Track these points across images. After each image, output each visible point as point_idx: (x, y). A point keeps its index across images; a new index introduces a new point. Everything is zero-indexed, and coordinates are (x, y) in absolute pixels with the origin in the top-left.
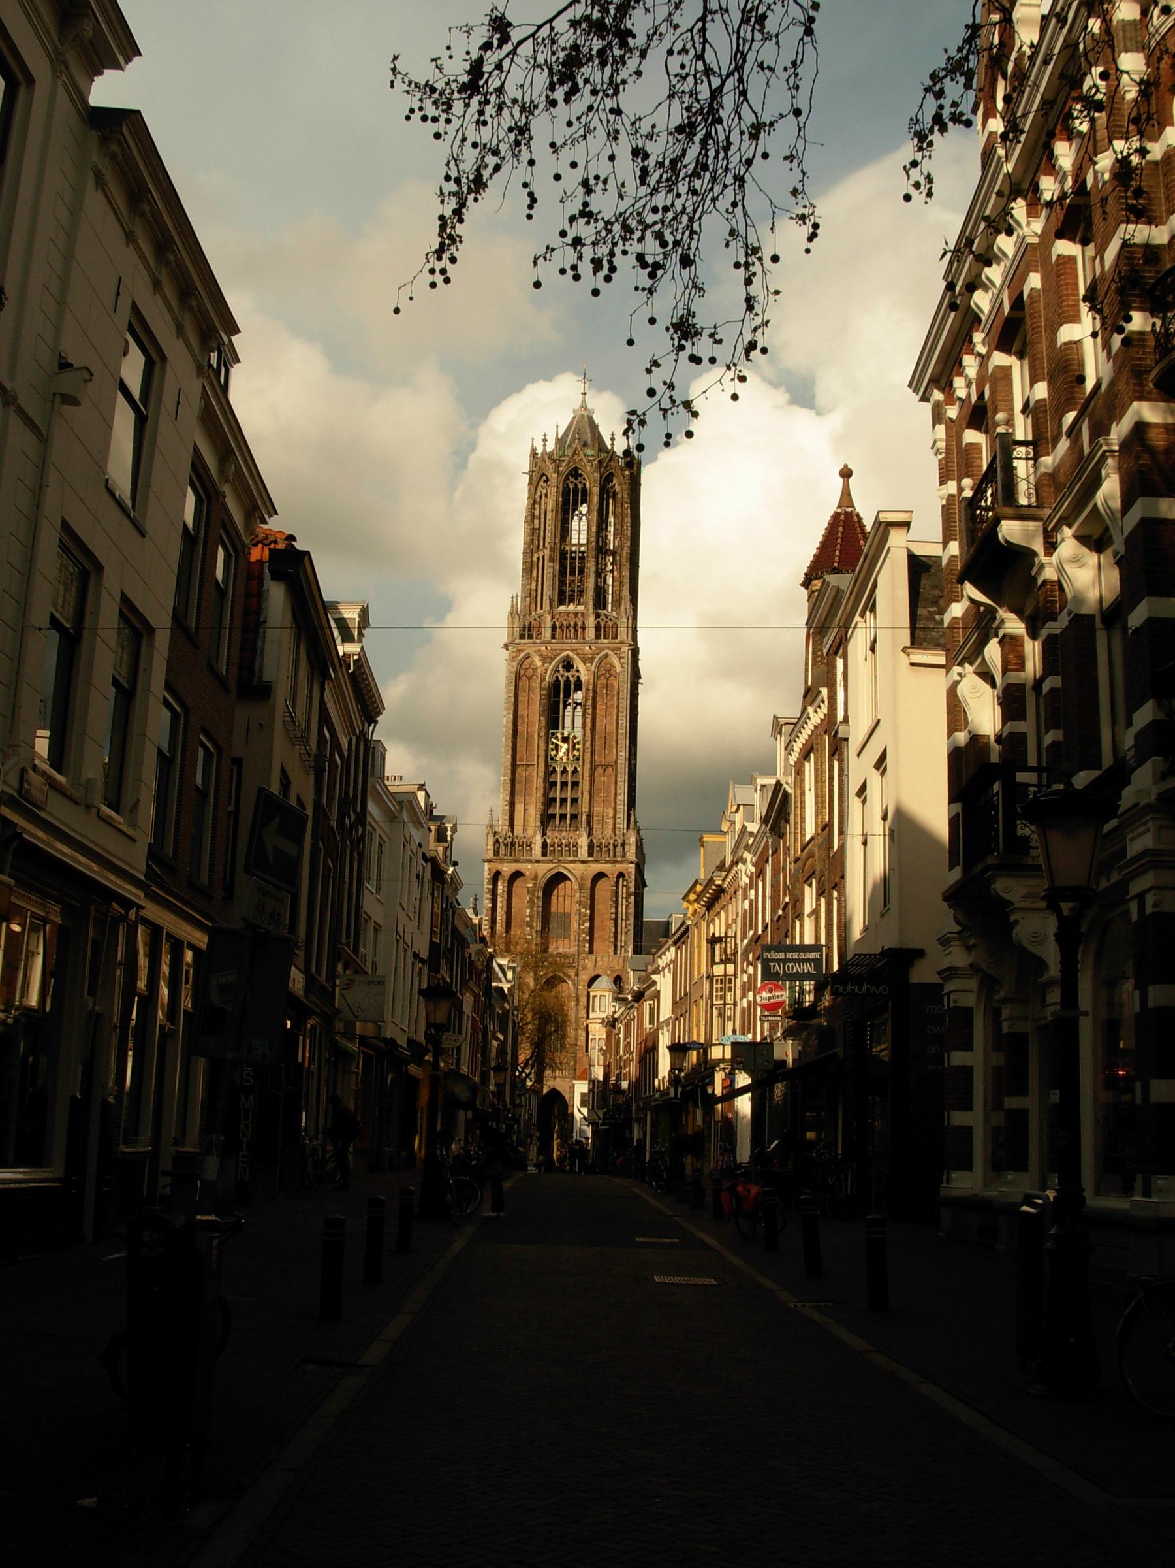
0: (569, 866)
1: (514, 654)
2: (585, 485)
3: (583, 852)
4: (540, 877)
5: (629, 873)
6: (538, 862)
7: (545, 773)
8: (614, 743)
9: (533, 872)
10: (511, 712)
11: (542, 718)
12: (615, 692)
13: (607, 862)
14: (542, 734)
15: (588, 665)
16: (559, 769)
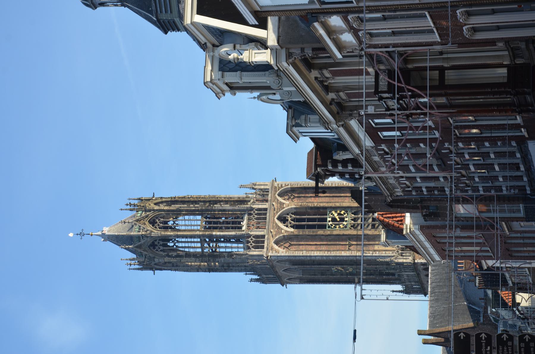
1: (274, 252)
16: (353, 222)
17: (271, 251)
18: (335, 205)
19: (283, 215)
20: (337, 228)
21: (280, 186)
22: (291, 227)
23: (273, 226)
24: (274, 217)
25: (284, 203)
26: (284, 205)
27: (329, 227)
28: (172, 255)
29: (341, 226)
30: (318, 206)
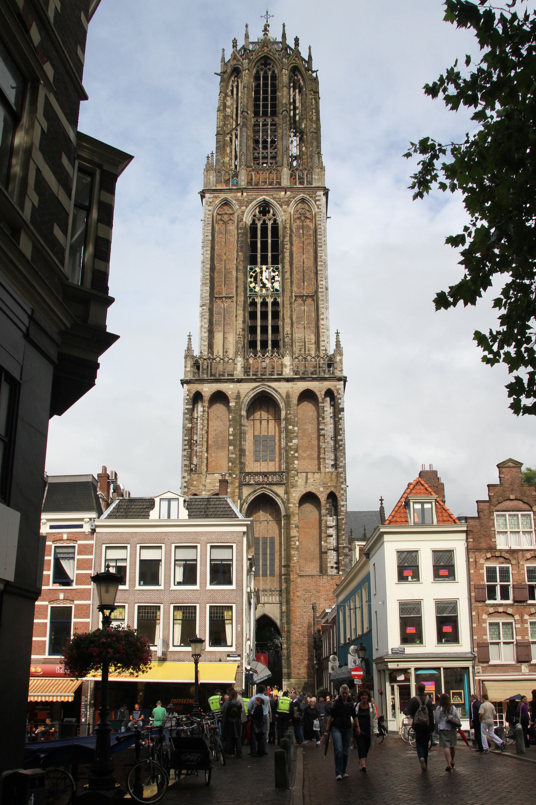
0: (273, 384)
1: (211, 200)
2: (274, 72)
3: (288, 372)
4: (242, 396)
5: (338, 390)
6: (240, 381)
7: (245, 302)
8: (313, 275)
9: (236, 392)
10: (209, 248)
11: (240, 253)
12: (311, 232)
13: (314, 379)
14: (241, 267)
15: (284, 207)
16: (259, 300)
17: (212, 196)
18: (286, 272)
19: (273, 208)
20: (249, 280)
21: (317, 198)
22: (254, 221)
23: (252, 195)
24: (267, 195)
25: (288, 205)
26: (286, 206)
27: (251, 269)
28: (227, 101)
29: (252, 285)
30: (285, 250)
